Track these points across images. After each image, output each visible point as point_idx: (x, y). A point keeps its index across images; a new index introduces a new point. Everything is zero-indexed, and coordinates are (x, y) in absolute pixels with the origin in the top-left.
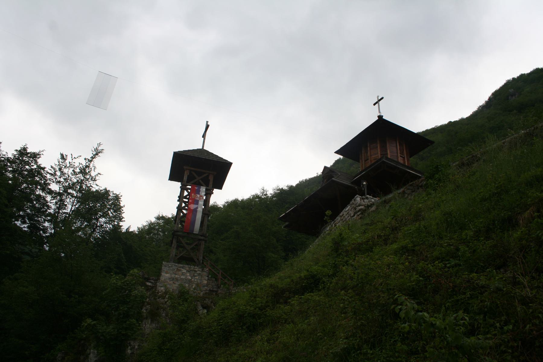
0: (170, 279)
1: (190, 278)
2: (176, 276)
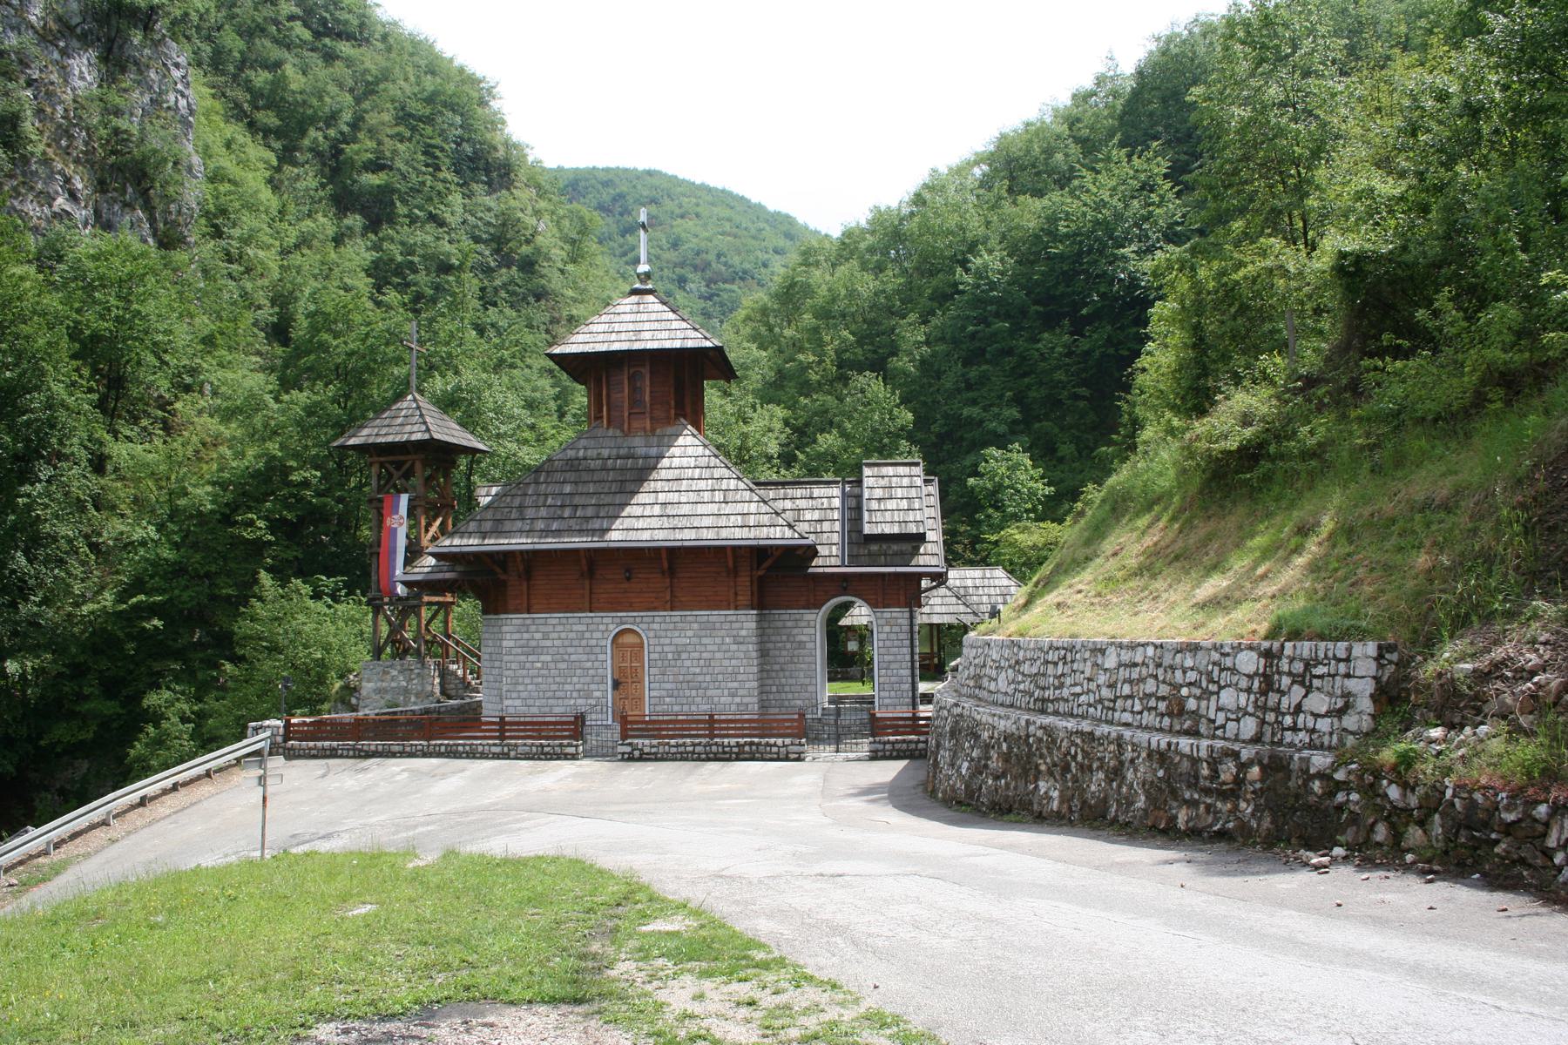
2: (384, 684)
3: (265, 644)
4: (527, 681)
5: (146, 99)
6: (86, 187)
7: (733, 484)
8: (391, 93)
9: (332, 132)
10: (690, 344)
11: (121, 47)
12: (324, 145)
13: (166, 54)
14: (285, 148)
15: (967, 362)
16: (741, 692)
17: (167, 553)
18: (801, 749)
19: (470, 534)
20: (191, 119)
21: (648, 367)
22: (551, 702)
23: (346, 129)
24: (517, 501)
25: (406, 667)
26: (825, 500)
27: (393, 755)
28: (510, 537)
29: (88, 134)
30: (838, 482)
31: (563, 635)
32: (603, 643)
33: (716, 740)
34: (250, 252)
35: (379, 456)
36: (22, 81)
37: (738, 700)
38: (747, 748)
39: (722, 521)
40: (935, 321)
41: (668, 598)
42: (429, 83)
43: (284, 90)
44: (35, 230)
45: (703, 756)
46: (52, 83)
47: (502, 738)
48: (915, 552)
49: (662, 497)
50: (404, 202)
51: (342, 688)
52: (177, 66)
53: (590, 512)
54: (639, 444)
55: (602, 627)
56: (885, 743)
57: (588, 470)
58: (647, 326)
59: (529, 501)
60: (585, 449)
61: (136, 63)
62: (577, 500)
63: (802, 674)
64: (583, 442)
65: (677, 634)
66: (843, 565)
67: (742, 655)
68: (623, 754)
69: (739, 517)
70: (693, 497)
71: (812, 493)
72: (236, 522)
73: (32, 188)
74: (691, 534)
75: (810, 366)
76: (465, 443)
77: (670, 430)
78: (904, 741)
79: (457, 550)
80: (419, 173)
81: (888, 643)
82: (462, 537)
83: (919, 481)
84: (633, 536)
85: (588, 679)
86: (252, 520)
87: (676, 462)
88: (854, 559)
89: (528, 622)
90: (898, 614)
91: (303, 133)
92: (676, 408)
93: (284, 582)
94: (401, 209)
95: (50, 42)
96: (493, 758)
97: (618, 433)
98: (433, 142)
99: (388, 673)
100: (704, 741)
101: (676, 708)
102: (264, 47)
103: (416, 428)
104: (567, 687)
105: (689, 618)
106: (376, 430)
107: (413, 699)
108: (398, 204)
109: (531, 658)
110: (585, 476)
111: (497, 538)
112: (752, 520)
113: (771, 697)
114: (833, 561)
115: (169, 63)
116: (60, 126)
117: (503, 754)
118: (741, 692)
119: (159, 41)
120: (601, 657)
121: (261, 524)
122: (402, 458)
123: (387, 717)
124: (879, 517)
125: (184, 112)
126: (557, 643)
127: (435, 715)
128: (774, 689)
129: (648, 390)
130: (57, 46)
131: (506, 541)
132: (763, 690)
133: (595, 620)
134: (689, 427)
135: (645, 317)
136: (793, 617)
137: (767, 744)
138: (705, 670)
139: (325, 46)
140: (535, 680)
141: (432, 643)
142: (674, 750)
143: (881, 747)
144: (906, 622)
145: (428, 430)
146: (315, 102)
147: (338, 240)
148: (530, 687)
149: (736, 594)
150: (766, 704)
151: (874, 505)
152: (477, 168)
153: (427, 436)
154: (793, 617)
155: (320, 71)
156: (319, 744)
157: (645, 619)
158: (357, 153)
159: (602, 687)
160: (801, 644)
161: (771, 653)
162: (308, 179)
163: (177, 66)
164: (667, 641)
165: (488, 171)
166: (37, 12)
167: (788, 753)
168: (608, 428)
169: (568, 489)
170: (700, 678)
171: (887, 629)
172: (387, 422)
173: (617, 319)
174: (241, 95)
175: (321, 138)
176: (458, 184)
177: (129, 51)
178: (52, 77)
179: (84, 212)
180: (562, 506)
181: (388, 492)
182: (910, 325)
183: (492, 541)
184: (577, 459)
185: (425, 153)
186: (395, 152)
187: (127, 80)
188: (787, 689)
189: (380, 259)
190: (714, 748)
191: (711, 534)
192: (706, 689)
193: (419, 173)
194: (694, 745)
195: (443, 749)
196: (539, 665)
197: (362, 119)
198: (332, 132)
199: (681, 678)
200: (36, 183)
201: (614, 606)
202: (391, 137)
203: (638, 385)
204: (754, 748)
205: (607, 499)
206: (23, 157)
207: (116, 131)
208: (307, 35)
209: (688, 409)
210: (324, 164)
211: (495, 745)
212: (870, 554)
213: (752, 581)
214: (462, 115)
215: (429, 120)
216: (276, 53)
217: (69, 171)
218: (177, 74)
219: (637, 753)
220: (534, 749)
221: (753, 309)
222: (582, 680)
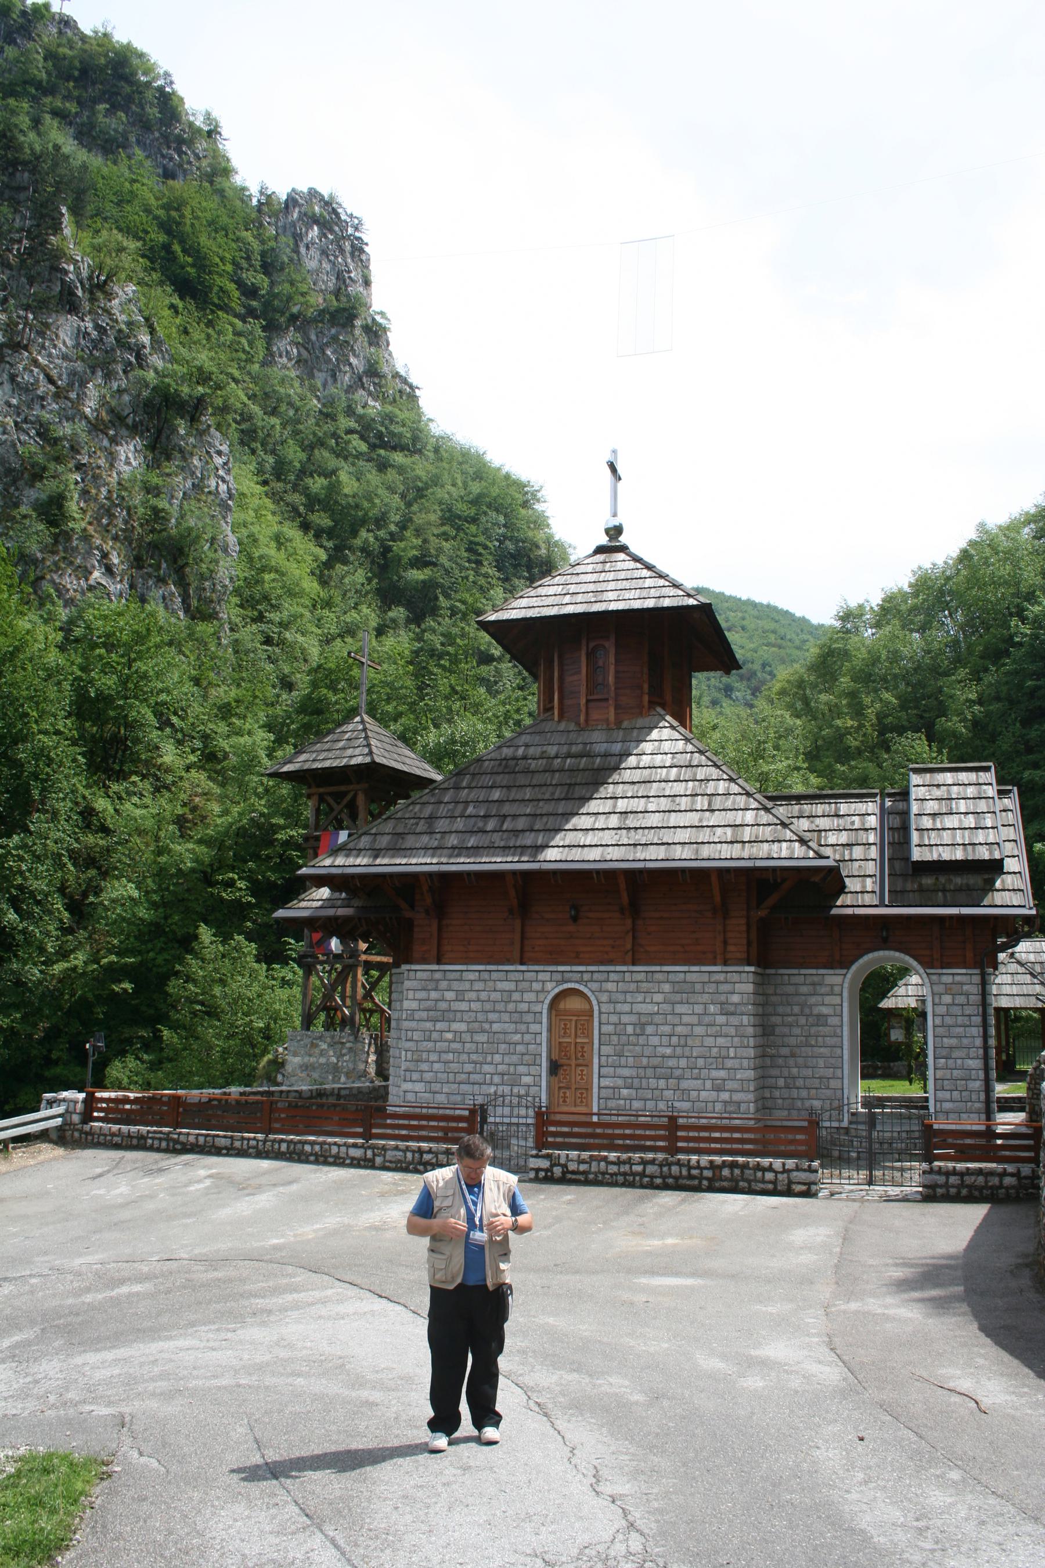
0: (301, 1067)
1: (335, 1061)
3: (199, 1007)
4: (433, 1057)
5: (189, 484)
6: (122, 562)
7: (722, 787)
8: (439, 496)
9: (381, 533)
10: (667, 603)
11: (168, 438)
12: (375, 546)
13: (209, 443)
14: (338, 549)
15: (1026, 723)
16: (730, 1085)
17: (142, 913)
18: (812, 1177)
19: (359, 852)
20: (230, 502)
21: (613, 640)
22: (465, 1088)
23: (393, 528)
24: (428, 811)
25: (337, 1039)
26: (856, 819)
27: (216, 1151)
28: (410, 856)
29: (129, 513)
30: (874, 795)
31: (483, 996)
32: (537, 1008)
33: (681, 1157)
34: (288, 635)
35: (318, 786)
36: (70, 465)
37: (725, 1096)
38: (726, 1172)
39: (704, 836)
40: (989, 679)
41: (629, 946)
42: (476, 488)
43: (338, 493)
44: (69, 603)
45: (658, 1181)
46: (99, 467)
47: (367, 1136)
48: (989, 887)
49: (622, 805)
50: (447, 596)
51: (270, 1062)
52: (219, 453)
53: (521, 823)
54: (598, 741)
55: (536, 986)
56: (948, 1174)
57: (527, 771)
58: (612, 586)
59: (443, 810)
60: (527, 746)
61: (181, 451)
62: (507, 809)
63: (821, 1062)
64: (525, 739)
65: (640, 998)
66: (882, 904)
67: (732, 1031)
68: (537, 1170)
69: (729, 831)
70: (664, 804)
71: (837, 809)
72: (217, 882)
73: (71, 563)
74: (661, 853)
75: (848, 731)
76: (418, 772)
77: (640, 722)
78: (980, 1172)
79: (339, 871)
80: (462, 568)
81: (948, 1020)
82: (347, 856)
83: (991, 791)
84: (576, 854)
85: (515, 1059)
86: (232, 879)
87: (646, 760)
88: (898, 897)
89: (437, 976)
90: (964, 978)
91: (355, 533)
92: (649, 694)
93: (225, 937)
94: (443, 602)
95: (101, 431)
96: (351, 1165)
97: (572, 726)
98: (477, 540)
99: (317, 1046)
100: (660, 1156)
101: (637, 1105)
102: (323, 457)
103: (357, 751)
104: (487, 1068)
105: (657, 976)
106: (314, 755)
107: (343, 1079)
108: (441, 598)
109: (439, 1026)
110: (522, 780)
111: (393, 857)
112: (747, 834)
113: (777, 1094)
114: (868, 899)
115: (212, 451)
116: (103, 506)
117: (365, 1160)
118: (730, 1085)
119: (204, 431)
120: (534, 1028)
121: (241, 884)
122: (343, 788)
123: (259, 1097)
124: (933, 838)
125: (224, 496)
126: (474, 1006)
127: (332, 1100)
128: (781, 1082)
129: (612, 668)
130: (107, 435)
131: (404, 861)
132: (763, 1083)
133: (528, 975)
134: (668, 718)
135: (611, 576)
136: (809, 980)
137: (758, 1167)
138: (679, 1051)
139: (379, 455)
140: (444, 1057)
141: (372, 1012)
142: (613, 1169)
143: (941, 1180)
144: (975, 989)
145: (371, 753)
146: (366, 504)
147: (380, 631)
148: (436, 1066)
149: (725, 943)
150: (769, 1103)
151: (927, 822)
152: (519, 565)
153: (368, 760)
154: (809, 980)
155: (373, 477)
156: (124, 1128)
157: (596, 976)
158: (404, 550)
159: (533, 1070)
160: (821, 1020)
161: (778, 1030)
162: (357, 576)
163: (219, 453)
164: (626, 1008)
165: (529, 568)
166: (92, 404)
167: (790, 1182)
168: (559, 721)
169: (496, 795)
170: (672, 1063)
171: (947, 999)
172: (327, 746)
173: (575, 579)
174: (297, 498)
175: (372, 539)
176: (499, 579)
177: (175, 439)
178: (100, 461)
179: (119, 586)
180: (486, 817)
181: (325, 829)
182: (960, 682)
183: (386, 861)
184: (514, 758)
185: (468, 550)
186: (440, 550)
187: (169, 467)
188: (800, 1083)
189: (421, 649)
190: (675, 1169)
191: (687, 853)
192: (678, 1078)
193: (462, 568)
194: (644, 1162)
195: (284, 1147)
196: (449, 1036)
197: (411, 520)
198: (381, 533)
199: (645, 1061)
200: (76, 558)
201: (554, 957)
202: (437, 536)
203: (600, 663)
204: (737, 1171)
205: (546, 808)
206: (66, 533)
207: (156, 511)
208: (363, 447)
209: (668, 697)
210: (373, 562)
211: (355, 1146)
212: (921, 890)
213: (748, 925)
214: (506, 516)
215: (474, 520)
216: (332, 462)
217: (106, 547)
218: (219, 461)
219: (557, 1171)
220: (409, 1155)
221: (788, 681)
222: (507, 1059)
